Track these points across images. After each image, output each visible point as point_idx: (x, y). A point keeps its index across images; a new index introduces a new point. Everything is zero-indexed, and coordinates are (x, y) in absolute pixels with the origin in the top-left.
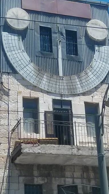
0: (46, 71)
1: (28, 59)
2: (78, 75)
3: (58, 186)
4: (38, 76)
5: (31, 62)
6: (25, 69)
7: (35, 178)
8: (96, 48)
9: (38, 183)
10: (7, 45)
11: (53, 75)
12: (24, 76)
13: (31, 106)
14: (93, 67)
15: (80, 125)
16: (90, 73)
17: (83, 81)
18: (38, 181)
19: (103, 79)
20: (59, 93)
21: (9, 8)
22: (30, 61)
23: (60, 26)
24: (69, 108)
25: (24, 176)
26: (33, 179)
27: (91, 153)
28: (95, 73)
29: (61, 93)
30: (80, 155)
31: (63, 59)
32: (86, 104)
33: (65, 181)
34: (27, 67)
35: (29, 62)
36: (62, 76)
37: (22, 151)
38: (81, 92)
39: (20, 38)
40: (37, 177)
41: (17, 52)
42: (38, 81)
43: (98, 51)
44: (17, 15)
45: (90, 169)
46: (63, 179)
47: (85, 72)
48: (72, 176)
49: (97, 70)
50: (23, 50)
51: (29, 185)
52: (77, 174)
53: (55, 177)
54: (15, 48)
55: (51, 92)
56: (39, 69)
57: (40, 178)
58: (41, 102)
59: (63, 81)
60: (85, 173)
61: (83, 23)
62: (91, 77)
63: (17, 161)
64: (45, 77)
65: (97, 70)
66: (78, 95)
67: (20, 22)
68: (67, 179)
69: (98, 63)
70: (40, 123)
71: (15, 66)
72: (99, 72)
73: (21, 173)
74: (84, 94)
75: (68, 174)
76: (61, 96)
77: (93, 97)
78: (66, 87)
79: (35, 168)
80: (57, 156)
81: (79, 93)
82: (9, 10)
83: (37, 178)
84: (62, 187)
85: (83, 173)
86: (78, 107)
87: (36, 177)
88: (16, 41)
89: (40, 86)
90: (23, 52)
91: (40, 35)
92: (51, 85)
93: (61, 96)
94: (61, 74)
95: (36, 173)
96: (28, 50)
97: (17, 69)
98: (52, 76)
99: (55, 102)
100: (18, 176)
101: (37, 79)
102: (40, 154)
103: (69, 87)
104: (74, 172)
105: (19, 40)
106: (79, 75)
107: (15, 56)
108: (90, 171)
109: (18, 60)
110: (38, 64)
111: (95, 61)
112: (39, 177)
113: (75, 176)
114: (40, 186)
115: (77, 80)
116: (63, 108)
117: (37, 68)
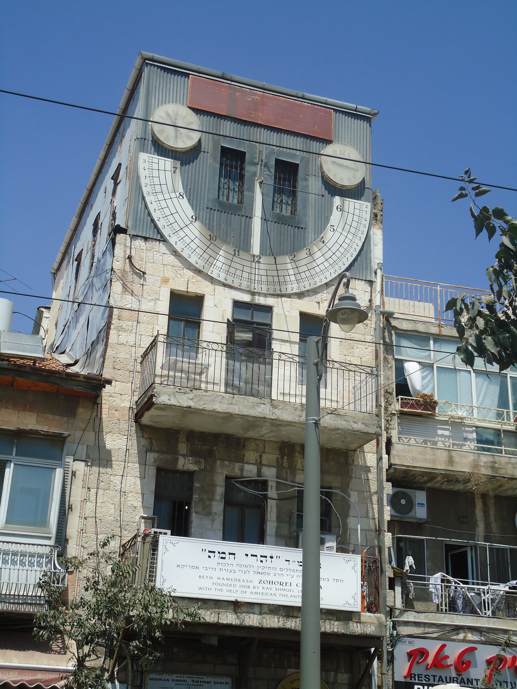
0: (225, 241)
1: (190, 212)
2: (293, 256)
3: (228, 478)
4: (208, 251)
5: (196, 219)
6: (182, 234)
7: (180, 457)
9: (185, 468)
10: (148, 181)
11: (238, 251)
12: (178, 248)
13: (186, 310)
14: (326, 241)
15: (283, 357)
16: (318, 254)
17: (301, 269)
18: (186, 464)
20: (248, 289)
21: (158, 103)
22: (194, 217)
23: (263, 149)
24: (269, 322)
25: (157, 452)
26: (177, 459)
27: (300, 417)
28: (330, 253)
29: (252, 290)
30: (274, 418)
31: (264, 219)
32: (303, 315)
33: (242, 470)
34: (186, 230)
35: (191, 219)
37: (154, 400)
38: (295, 291)
40: (184, 456)
41: (167, 196)
42: (206, 261)
43: (339, 210)
44: (176, 119)
46: (237, 465)
47: (308, 250)
48: (259, 460)
49: (334, 249)
50: (182, 194)
51: (167, 471)
52: (270, 457)
53: (223, 460)
54: (164, 187)
55: (233, 285)
56: (210, 235)
57: (191, 458)
58: (207, 303)
59: (259, 266)
60: (285, 457)
61: (314, 146)
62: (319, 262)
63: (145, 420)
64: (221, 253)
65: (334, 249)
66: (289, 296)
67: (181, 134)
68: (247, 467)
69: (337, 234)
70: (200, 346)
71: (160, 224)
72: (338, 254)
73: (152, 445)
74: (300, 295)
75: (251, 455)
76: (253, 294)
77: (319, 303)
78: (264, 278)
79: (182, 438)
80: (229, 417)
81: (292, 292)
82: (158, 107)
83: (185, 459)
84: (236, 482)
85: (282, 458)
86: (285, 319)
87: (182, 455)
88: (169, 174)
90: (181, 197)
91: (221, 164)
92: (232, 270)
93: (253, 294)
94: (256, 249)
95: (183, 448)
96: (191, 194)
97: (166, 232)
98: (237, 253)
99: (237, 304)
100: (145, 450)
101: (206, 256)
102: (192, 410)
103: (270, 279)
105: (174, 172)
106: (295, 256)
107: (163, 203)
109: (167, 212)
110: (208, 225)
111: (332, 230)
112: (188, 457)
113: (264, 462)
114: (191, 474)
115: (289, 266)
116: (255, 320)
117: (207, 233)
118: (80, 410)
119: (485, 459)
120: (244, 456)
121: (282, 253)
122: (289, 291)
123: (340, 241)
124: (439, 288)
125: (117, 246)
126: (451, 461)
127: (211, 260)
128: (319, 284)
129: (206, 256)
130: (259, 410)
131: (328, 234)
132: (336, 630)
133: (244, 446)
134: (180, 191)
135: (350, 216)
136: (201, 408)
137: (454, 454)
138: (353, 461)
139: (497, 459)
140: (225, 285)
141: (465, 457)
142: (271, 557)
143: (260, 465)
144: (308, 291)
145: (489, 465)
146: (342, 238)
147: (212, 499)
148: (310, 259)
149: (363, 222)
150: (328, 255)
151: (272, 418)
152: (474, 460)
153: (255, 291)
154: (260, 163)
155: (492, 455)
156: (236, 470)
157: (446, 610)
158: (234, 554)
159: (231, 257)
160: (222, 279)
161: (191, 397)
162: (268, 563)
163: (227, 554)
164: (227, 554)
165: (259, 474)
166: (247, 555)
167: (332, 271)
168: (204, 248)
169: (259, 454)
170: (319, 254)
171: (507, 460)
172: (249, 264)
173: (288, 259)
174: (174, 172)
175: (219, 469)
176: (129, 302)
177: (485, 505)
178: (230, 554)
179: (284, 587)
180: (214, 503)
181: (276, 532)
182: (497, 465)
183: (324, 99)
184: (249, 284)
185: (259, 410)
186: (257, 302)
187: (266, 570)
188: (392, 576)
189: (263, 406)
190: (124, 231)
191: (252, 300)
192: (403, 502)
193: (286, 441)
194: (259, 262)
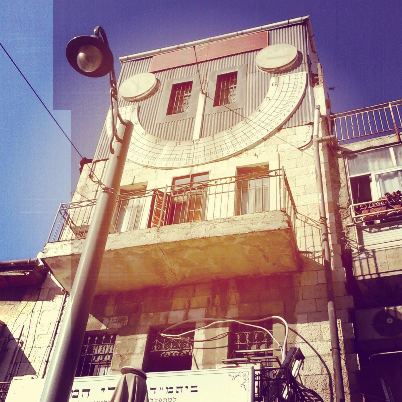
4: (154, 150)
19: (280, 122)
20: (187, 165)
22: (144, 133)
28: (266, 116)
29: (190, 164)
33: (167, 318)
39: (134, 109)
45: (232, 284)
46: (162, 314)
48: (187, 306)
53: (147, 313)
57: (115, 318)
60: (217, 297)
65: (269, 113)
68: (172, 314)
69: (273, 102)
75: (179, 301)
83: (110, 319)
85: (214, 297)
87: (107, 317)
89: (154, 164)
92: (173, 157)
98: (178, 144)
101: (151, 154)
103: (207, 152)
104: (194, 296)
105: (132, 112)
106: (231, 129)
108: (231, 290)
117: (153, 139)
120: (172, 304)
123: (276, 105)
124: (390, 106)
125: (82, 173)
127: (155, 156)
128: (255, 141)
131: (265, 105)
133: (172, 296)
134: (135, 121)
138: (299, 283)
140: (167, 169)
144: (246, 150)
146: (278, 102)
147: (131, 354)
148: (247, 126)
151: (156, 242)
153: (193, 164)
154: (204, 82)
158: (89, 390)
159: (172, 148)
160: (163, 166)
161: (76, 245)
163: (81, 391)
164: (81, 391)
165: (186, 317)
166: (103, 389)
168: (150, 149)
169: (187, 299)
172: (188, 148)
173: (225, 133)
174: (132, 112)
175: (143, 323)
178: (84, 391)
180: (133, 357)
184: (187, 161)
190: (90, 161)
193: (214, 277)
194: (198, 144)
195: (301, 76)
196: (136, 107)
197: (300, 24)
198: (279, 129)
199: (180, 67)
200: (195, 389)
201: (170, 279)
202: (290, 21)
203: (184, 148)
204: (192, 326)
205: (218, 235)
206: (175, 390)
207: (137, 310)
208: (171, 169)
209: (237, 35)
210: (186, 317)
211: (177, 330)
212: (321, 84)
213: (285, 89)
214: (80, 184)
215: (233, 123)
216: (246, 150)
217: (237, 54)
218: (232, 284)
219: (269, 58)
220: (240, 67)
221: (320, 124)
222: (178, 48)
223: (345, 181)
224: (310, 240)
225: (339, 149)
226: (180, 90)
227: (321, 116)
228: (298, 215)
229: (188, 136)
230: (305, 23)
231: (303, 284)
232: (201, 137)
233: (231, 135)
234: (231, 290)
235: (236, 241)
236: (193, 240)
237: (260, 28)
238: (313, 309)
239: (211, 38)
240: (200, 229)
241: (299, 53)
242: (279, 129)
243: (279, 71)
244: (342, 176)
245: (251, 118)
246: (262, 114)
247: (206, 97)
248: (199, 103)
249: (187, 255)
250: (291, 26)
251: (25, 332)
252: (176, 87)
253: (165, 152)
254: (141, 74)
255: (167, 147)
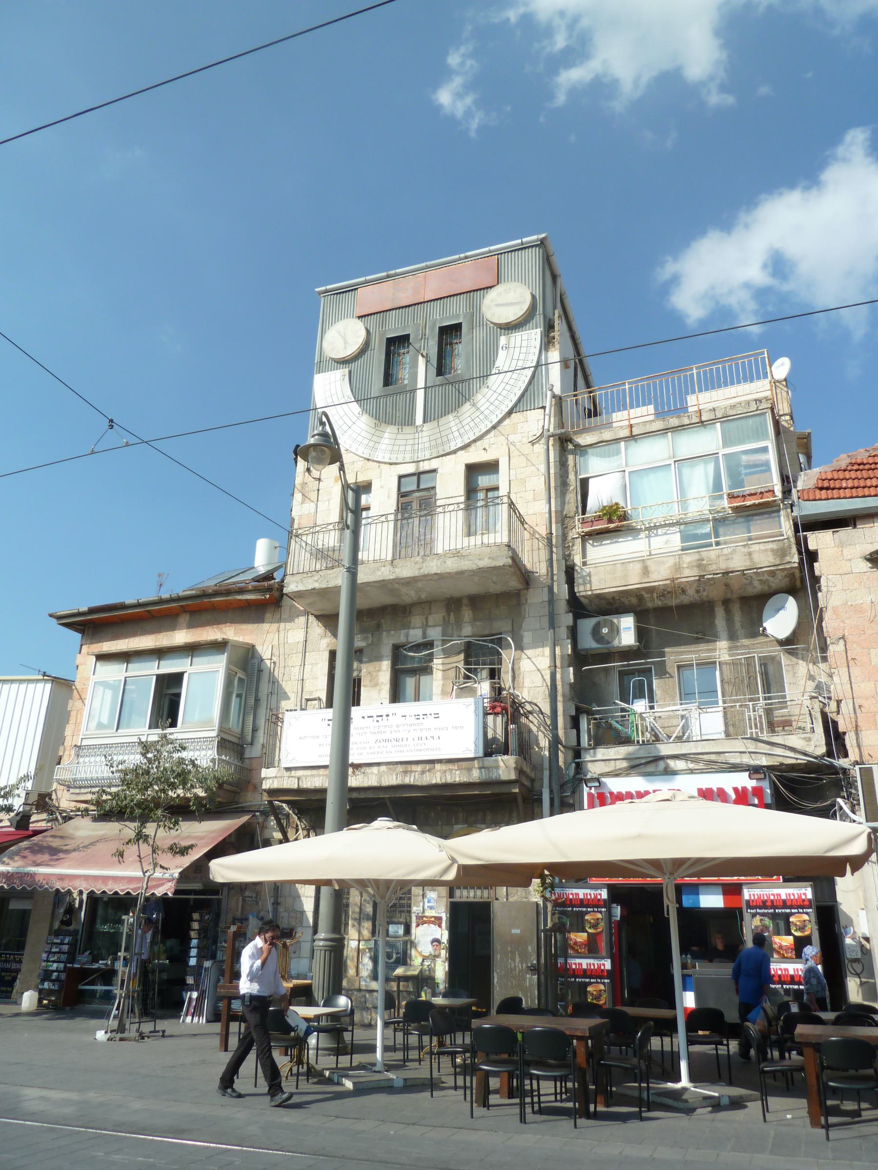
3: (396, 648)
8: (503, 340)
14: (490, 385)
17: (464, 423)
19: (511, 405)
28: (496, 395)
33: (407, 636)
34: (354, 427)
36: (421, 423)
45: (465, 601)
46: (403, 632)
52: (437, 616)
60: (452, 614)
64: (386, 435)
65: (499, 391)
66: (454, 452)
68: (412, 632)
85: (449, 615)
88: (338, 384)
103: (433, 443)
108: (464, 608)
113: (431, 623)
117: (372, 421)
118: (268, 615)
119: (690, 558)
121: (445, 413)
122: (453, 448)
126: (646, 571)
129: (372, 444)
130: (379, 573)
132: (457, 780)
135: (517, 350)
136: (324, 586)
137: (649, 563)
138: (526, 600)
139: (704, 555)
140: (391, 464)
141: (664, 563)
142: (388, 716)
143: (425, 627)
144: (475, 441)
145: (695, 564)
147: (379, 671)
149: (532, 350)
150: (492, 400)
151: (392, 577)
152: (675, 564)
155: (699, 552)
156: (400, 637)
157: (643, 741)
159: (394, 436)
161: (316, 578)
162: (384, 722)
167: (498, 412)
170: (484, 400)
171: (717, 552)
172: (412, 436)
173: (450, 417)
176: (309, 507)
177: (728, 611)
179: (401, 743)
180: (381, 674)
181: (442, 690)
182: (704, 562)
183: (486, 249)
185: (379, 573)
186: (421, 469)
187: (382, 729)
188: (574, 714)
189: (383, 569)
191: (417, 469)
192: (605, 631)
194: (422, 431)
195: (533, 336)
196: (346, 371)
197: (536, 246)
198: (510, 413)
199: (393, 309)
200: (437, 716)
201: (407, 600)
202: (524, 240)
203: (408, 437)
204: (430, 645)
205: (448, 571)
206: (421, 717)
207: (378, 627)
208: (396, 464)
209: (460, 259)
210: (424, 635)
211: (418, 647)
212: (557, 346)
213: (516, 357)
214: (298, 480)
215: (459, 405)
216: (475, 441)
217: (460, 294)
218: (465, 601)
219: (498, 305)
220: (465, 317)
221: (553, 408)
222: (388, 276)
223: (574, 484)
224: (535, 560)
225: (571, 440)
226: (397, 344)
227: (554, 396)
228: (526, 526)
229: (409, 421)
230: (542, 243)
231: (529, 601)
232: (424, 422)
233: (457, 421)
234: (464, 608)
235: (466, 575)
236: (425, 576)
237: (486, 249)
238: (538, 626)
239: (428, 263)
240: (432, 564)
241: (533, 297)
242: (510, 413)
243: (510, 327)
244: (572, 476)
245: (479, 396)
246: (491, 392)
247: (427, 362)
248: (419, 370)
249: (420, 585)
250: (525, 248)
251: (276, 652)
252: (391, 342)
253: (386, 441)
254: (346, 320)
255: (389, 432)
